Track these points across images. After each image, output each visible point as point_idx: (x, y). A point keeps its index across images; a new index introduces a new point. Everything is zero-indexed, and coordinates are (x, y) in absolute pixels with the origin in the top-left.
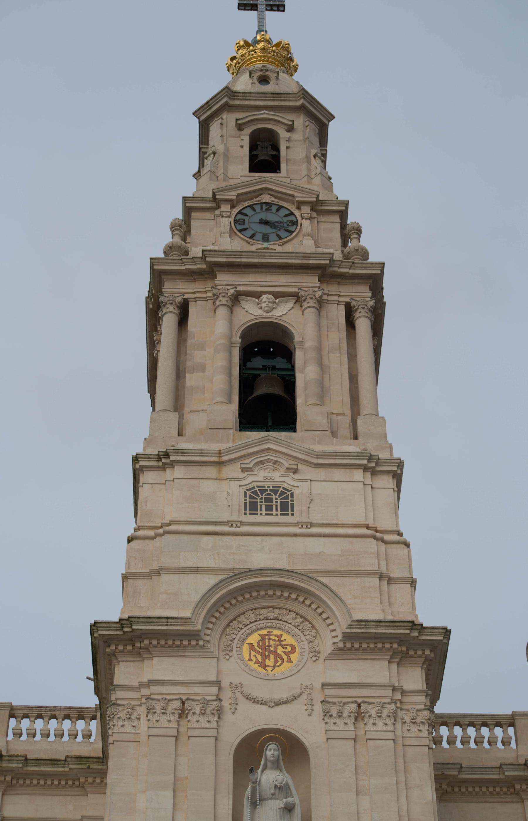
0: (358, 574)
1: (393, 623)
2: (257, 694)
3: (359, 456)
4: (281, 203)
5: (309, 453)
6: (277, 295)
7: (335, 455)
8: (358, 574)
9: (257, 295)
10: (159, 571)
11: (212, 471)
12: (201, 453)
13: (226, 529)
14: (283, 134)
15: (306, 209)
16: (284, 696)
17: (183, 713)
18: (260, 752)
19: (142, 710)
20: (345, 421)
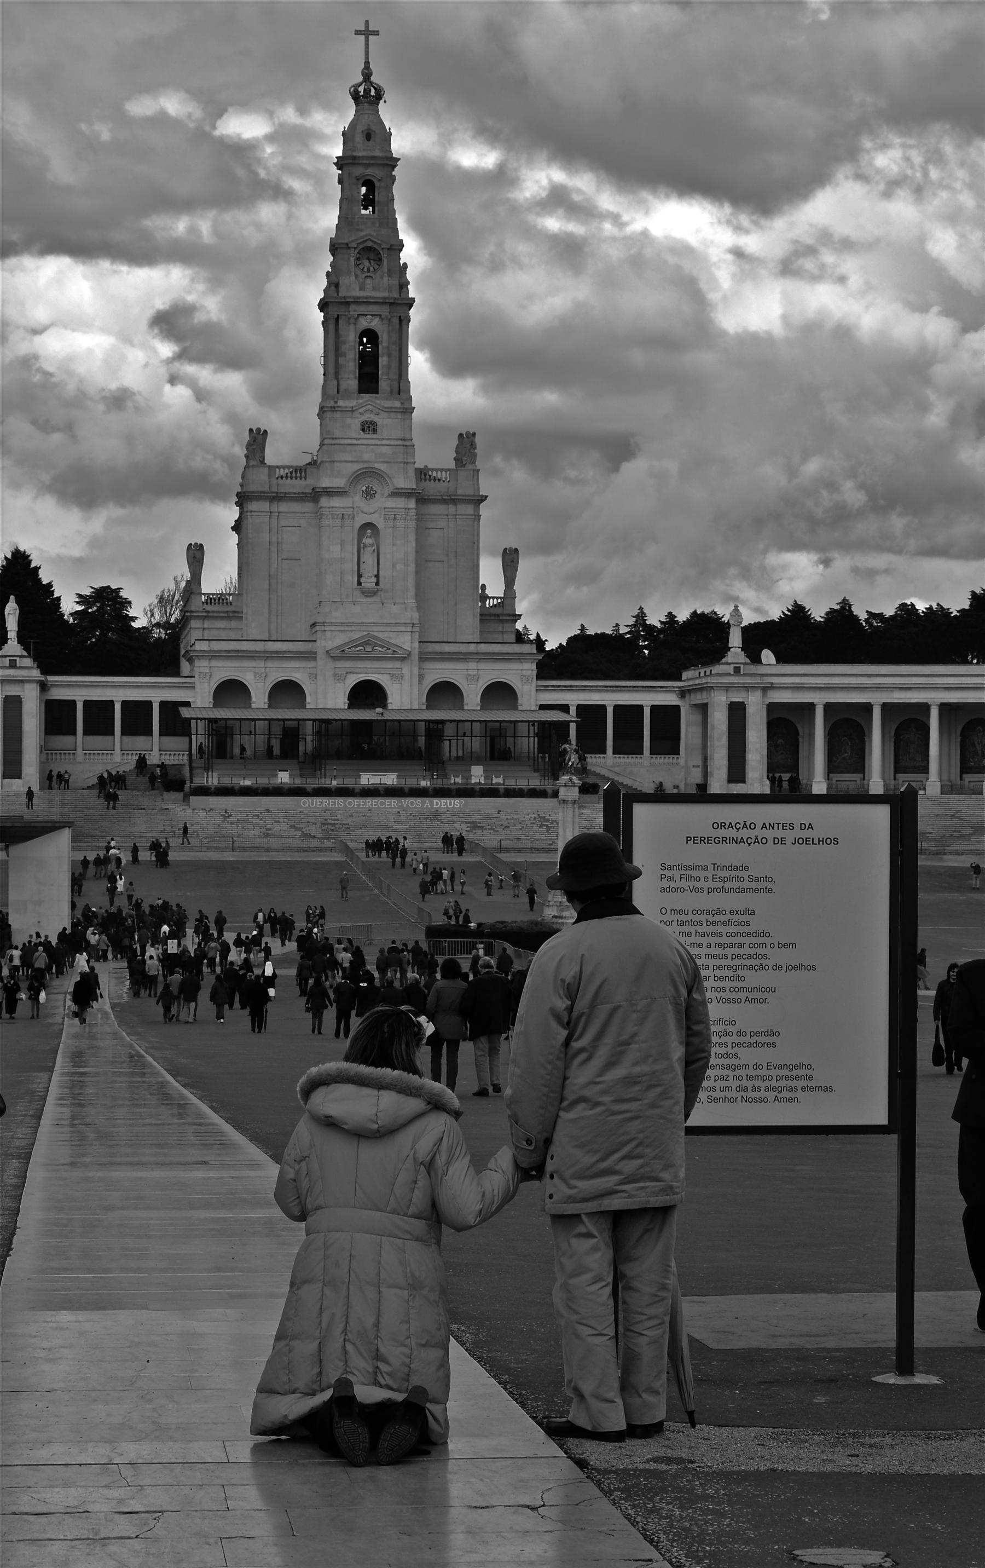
0: (397, 462)
1: (407, 489)
2: (365, 510)
3: (400, 408)
4: (375, 246)
5: (383, 407)
6: (372, 315)
7: (391, 408)
8: (397, 462)
9: (366, 315)
10: (334, 462)
11: (350, 413)
12: (346, 407)
13: (354, 442)
14: (377, 184)
15: (386, 251)
16: (372, 511)
17: (343, 518)
18: (365, 533)
19: (330, 516)
20: (396, 384)
